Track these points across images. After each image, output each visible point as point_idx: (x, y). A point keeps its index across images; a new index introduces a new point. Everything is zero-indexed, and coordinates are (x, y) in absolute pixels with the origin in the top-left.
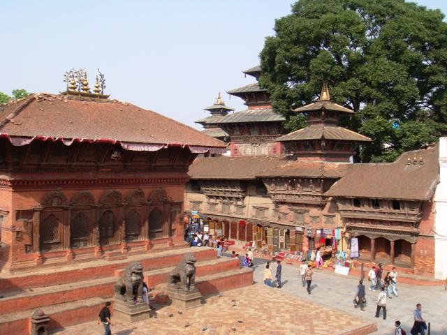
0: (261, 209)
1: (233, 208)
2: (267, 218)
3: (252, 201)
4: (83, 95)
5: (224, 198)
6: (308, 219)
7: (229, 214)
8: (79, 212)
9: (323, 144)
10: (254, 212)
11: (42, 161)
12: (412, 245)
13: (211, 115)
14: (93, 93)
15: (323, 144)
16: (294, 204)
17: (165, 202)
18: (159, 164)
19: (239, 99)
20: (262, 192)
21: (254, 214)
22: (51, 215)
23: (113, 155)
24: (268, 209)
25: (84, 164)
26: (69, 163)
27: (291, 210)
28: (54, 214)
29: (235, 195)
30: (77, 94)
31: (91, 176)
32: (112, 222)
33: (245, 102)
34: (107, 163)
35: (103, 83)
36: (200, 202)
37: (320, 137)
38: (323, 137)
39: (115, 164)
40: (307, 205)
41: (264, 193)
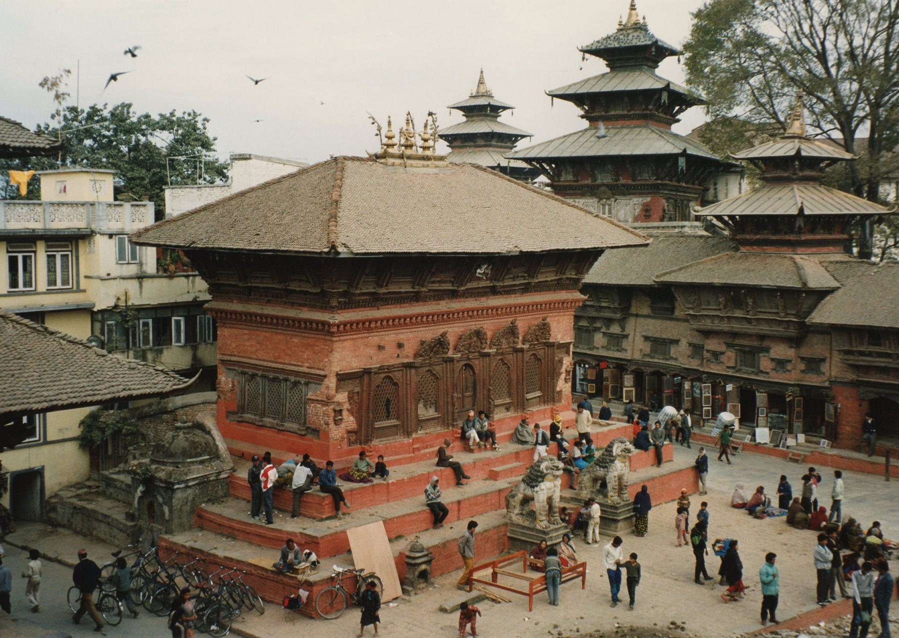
0: (660, 344)
2: (676, 359)
6: (765, 363)
10: (647, 347)
13: (464, 119)
15: (800, 222)
16: (735, 335)
18: (541, 278)
19: (570, 105)
20: (666, 309)
26: (417, 289)
29: (607, 314)
31: (444, 306)
32: (470, 385)
33: (582, 113)
38: (801, 210)
40: (762, 337)
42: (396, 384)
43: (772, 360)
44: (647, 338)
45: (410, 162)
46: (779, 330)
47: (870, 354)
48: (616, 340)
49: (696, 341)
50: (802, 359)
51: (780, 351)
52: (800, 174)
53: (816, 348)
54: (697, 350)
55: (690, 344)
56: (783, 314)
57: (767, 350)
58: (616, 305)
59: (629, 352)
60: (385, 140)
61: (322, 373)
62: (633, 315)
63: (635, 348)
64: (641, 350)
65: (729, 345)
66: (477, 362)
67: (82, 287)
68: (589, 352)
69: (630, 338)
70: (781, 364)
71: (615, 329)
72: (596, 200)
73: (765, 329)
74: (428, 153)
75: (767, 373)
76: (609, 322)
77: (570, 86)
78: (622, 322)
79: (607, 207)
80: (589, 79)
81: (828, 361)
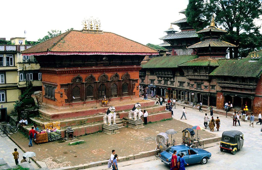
0: (181, 83)
1: (169, 83)
3: (179, 79)
4: (90, 31)
5: (164, 77)
6: (203, 87)
7: (167, 85)
8: (89, 84)
9: (210, 49)
10: (178, 84)
11: (71, 62)
12: (252, 101)
13: (167, 35)
14: (96, 29)
15: (210, 49)
16: (196, 80)
17: (130, 80)
21: (179, 85)
22: (76, 86)
23: (103, 58)
24: (185, 82)
25: (90, 63)
27: (195, 83)
28: (78, 86)
29: (170, 76)
30: (88, 30)
32: (104, 89)
34: (102, 62)
35: (100, 24)
36: (155, 80)
37: (208, 46)
39: (105, 62)
40: (202, 80)
41: (182, 75)
42: (79, 88)
43: (204, 86)
44: (179, 82)
45: (90, 32)
46: (205, 78)
47: (224, 83)
48: (172, 82)
49: (188, 82)
50: (211, 85)
51: (206, 84)
52: (213, 37)
53: (214, 82)
54: (189, 84)
55: (187, 83)
56: (205, 74)
57: (203, 83)
58: (171, 73)
59: (175, 85)
60: (85, 27)
61: (56, 84)
62: (176, 76)
63: (176, 85)
64: (178, 85)
65: (195, 83)
66: (106, 83)
67: (16, 66)
68: (167, 86)
69: (175, 82)
70: (206, 87)
71: (172, 80)
72: (182, 50)
73: (202, 78)
74: (99, 29)
75: (203, 90)
76: (171, 78)
77: (176, 22)
78: (173, 78)
79: (185, 51)
80: (181, 20)
81: (216, 85)
